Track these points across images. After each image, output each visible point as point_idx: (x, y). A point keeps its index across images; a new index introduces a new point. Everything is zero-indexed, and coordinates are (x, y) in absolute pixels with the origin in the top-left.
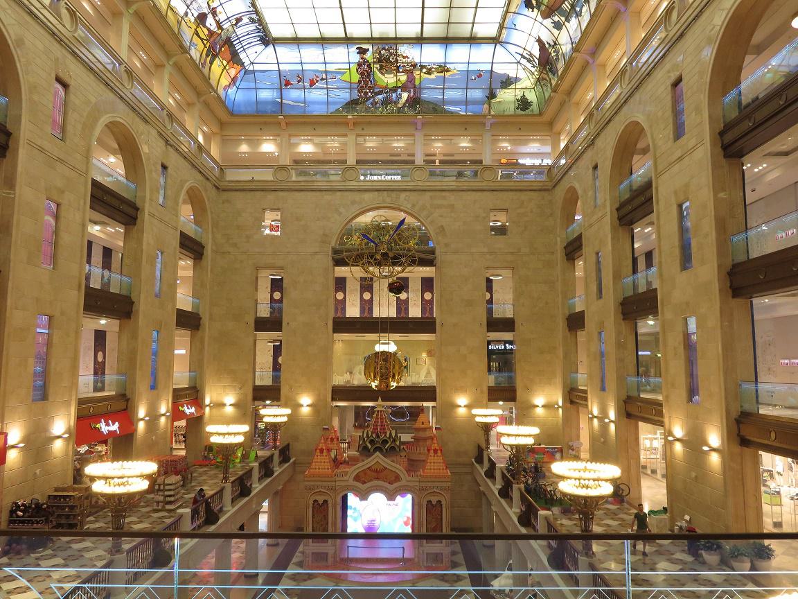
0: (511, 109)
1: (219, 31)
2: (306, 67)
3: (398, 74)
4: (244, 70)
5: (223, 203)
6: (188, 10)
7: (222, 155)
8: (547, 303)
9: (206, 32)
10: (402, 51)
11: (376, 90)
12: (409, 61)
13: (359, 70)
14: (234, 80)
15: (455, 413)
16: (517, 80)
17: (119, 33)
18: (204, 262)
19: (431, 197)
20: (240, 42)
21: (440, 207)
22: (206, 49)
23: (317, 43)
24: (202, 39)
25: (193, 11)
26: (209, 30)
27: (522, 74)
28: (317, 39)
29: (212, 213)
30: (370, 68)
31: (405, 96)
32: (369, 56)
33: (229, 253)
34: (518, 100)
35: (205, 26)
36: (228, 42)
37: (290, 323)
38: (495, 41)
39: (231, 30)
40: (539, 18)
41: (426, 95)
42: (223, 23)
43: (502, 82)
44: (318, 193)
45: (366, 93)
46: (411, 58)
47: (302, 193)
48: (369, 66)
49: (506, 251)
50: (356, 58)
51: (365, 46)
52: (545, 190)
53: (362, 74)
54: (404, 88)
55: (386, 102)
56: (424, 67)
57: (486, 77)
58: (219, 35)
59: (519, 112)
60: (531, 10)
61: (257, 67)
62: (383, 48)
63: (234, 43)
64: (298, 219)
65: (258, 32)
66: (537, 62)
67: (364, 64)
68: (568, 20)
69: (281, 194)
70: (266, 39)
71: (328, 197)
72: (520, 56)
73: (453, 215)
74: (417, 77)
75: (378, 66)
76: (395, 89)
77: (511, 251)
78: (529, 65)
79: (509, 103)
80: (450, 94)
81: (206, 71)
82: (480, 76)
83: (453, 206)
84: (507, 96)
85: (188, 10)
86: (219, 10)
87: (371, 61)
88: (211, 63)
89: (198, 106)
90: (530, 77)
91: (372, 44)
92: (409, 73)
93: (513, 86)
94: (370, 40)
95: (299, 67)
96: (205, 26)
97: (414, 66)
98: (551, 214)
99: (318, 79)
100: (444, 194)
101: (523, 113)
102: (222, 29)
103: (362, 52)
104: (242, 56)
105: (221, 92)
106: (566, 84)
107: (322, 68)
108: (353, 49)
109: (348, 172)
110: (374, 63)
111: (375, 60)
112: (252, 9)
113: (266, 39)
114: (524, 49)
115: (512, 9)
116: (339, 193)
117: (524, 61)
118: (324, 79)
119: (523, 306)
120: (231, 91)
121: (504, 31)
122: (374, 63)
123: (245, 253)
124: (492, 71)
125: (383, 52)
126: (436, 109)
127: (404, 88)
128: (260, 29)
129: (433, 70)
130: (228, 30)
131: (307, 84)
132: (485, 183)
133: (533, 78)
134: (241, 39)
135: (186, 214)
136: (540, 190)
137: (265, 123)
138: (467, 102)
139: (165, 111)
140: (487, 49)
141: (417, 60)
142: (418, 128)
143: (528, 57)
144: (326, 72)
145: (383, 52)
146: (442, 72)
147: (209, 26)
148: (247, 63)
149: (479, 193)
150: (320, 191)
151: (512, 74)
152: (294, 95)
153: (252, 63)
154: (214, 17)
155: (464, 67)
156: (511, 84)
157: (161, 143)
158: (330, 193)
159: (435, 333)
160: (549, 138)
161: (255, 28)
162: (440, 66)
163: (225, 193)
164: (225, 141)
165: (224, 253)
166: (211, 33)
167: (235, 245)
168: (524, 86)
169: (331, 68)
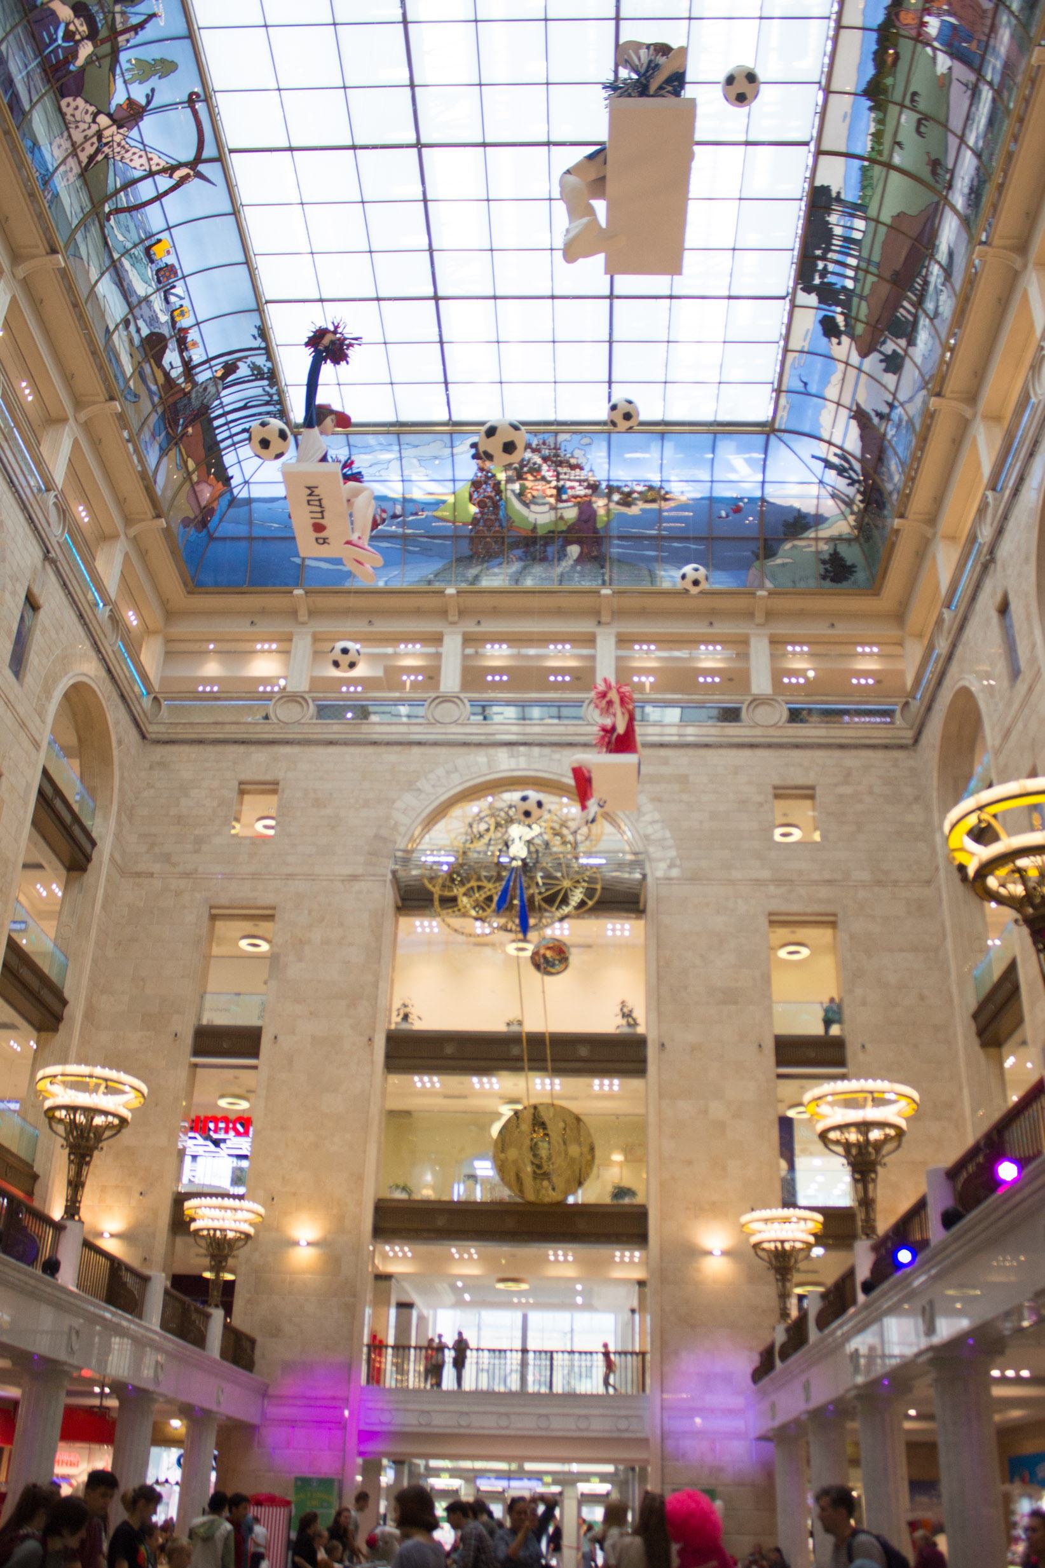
1: (188, 388)
3: (561, 505)
4: (228, 497)
5: (151, 768)
6: (130, 317)
7: (163, 680)
8: (922, 998)
9: (161, 379)
10: (569, 450)
12: (583, 475)
13: (475, 496)
16: (819, 520)
18: (89, 877)
20: (227, 424)
21: (655, 779)
23: (388, 433)
25: (141, 323)
26: (167, 375)
29: (122, 778)
33: (152, 875)
34: (824, 562)
36: (203, 416)
37: (280, 1038)
40: (855, 358)
42: (198, 370)
43: (786, 524)
44: (370, 750)
46: (587, 468)
47: (331, 750)
49: (815, 877)
50: (468, 469)
52: (901, 747)
53: (481, 504)
56: (618, 489)
58: (187, 394)
60: (834, 340)
61: (257, 492)
63: (216, 423)
64: (318, 803)
65: (267, 403)
66: (857, 466)
67: (486, 483)
68: (911, 342)
69: (287, 750)
71: (391, 756)
72: (822, 464)
73: (685, 797)
74: (601, 512)
77: (827, 875)
78: (841, 483)
82: (737, 510)
85: (130, 317)
86: (193, 335)
87: (501, 476)
90: (847, 511)
93: (811, 534)
96: (160, 365)
97: (594, 487)
98: (917, 799)
99: (384, 516)
100: (663, 752)
102: (195, 384)
104: (229, 459)
109: (440, 707)
110: (509, 480)
111: (510, 473)
112: (259, 343)
114: (830, 443)
116: (416, 751)
117: (831, 476)
118: (399, 517)
119: (864, 1003)
123: (187, 875)
128: (271, 396)
129: (635, 495)
130: (205, 389)
132: (758, 732)
133: (852, 513)
134: (230, 417)
136: (886, 747)
139: (52, 494)
142: (604, 619)
143: (836, 461)
146: (653, 501)
147: (168, 368)
149: (747, 753)
150: (375, 743)
153: (246, 482)
154: (181, 352)
156: (806, 527)
157: (37, 553)
158: (398, 749)
161: (260, 391)
162: (651, 488)
164: (169, 656)
165: (138, 875)
166: (169, 380)
167: (167, 858)
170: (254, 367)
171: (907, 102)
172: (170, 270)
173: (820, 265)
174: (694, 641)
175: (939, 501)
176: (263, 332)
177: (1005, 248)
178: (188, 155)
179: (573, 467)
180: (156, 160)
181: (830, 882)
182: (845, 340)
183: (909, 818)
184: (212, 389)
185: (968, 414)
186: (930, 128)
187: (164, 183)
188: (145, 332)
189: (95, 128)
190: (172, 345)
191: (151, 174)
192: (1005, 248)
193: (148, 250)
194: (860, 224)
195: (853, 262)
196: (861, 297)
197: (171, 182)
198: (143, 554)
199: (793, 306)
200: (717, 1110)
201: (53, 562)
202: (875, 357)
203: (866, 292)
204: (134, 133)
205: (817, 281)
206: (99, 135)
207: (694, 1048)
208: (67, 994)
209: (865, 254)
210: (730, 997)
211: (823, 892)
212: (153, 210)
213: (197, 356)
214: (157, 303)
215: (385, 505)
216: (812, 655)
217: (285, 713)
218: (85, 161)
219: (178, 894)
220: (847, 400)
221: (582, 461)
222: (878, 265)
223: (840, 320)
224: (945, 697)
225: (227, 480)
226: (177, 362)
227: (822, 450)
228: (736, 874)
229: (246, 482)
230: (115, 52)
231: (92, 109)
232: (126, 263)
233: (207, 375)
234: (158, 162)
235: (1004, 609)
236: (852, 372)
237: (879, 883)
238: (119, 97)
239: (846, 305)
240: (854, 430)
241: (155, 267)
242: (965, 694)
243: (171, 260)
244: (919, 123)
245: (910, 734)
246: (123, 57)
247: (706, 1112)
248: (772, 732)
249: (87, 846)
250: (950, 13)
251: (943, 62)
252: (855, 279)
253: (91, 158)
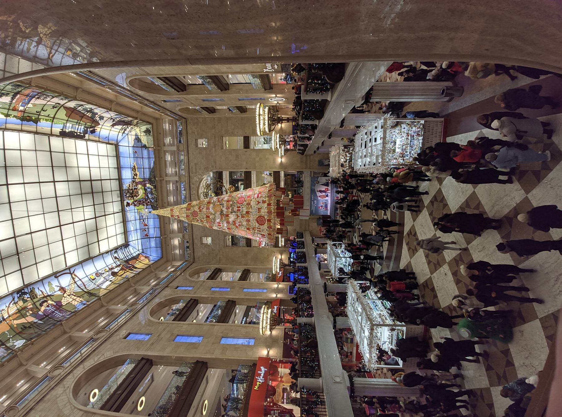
0: (151, 138)
1: (121, 266)
2: (138, 227)
7: (181, 260)
9: (121, 271)
11: (147, 198)
14: (146, 257)
16: (136, 135)
17: (115, 310)
19: (192, 173)
21: (196, 169)
22: (129, 271)
24: (124, 273)
26: (120, 270)
27: (133, 133)
28: (124, 224)
30: (136, 201)
31: (148, 185)
32: (130, 202)
33: (220, 258)
35: (118, 272)
36: (127, 261)
38: (117, 146)
39: (121, 261)
40: (100, 126)
41: (147, 176)
43: (138, 142)
45: (148, 202)
48: (135, 201)
50: (132, 207)
51: (125, 204)
52: (186, 122)
53: (140, 204)
54: (144, 186)
55: (152, 193)
57: (136, 149)
59: (151, 134)
61: (140, 248)
62: (126, 195)
66: (124, 126)
68: (97, 114)
69: (194, 237)
70: (126, 245)
74: (139, 180)
75: (135, 197)
76: (145, 190)
78: (128, 130)
79: (148, 139)
80: (146, 165)
81: (141, 270)
82: (136, 152)
83: (196, 164)
84: (145, 140)
86: (110, 267)
87: (133, 201)
88: (136, 268)
89: (157, 272)
91: (124, 201)
92: (137, 184)
93: (140, 137)
94: (122, 201)
95: (139, 231)
96: (118, 272)
97: (133, 182)
98: (197, 119)
100: (190, 168)
101: (152, 132)
102: (120, 264)
103: (128, 204)
104: (135, 255)
105: (152, 262)
106: (134, 114)
107: (138, 222)
108: (127, 208)
110: (133, 199)
113: (126, 245)
115: (97, 139)
117: (126, 132)
120: (151, 258)
121: (110, 142)
122: (133, 199)
124: (133, 147)
125: (128, 196)
126: (153, 171)
127: (144, 186)
131: (146, 227)
132: (185, 149)
135: (204, 276)
136: (187, 125)
137: (165, 244)
138: (149, 158)
140: (121, 149)
141: (131, 180)
143: (123, 131)
144: (140, 219)
145: (128, 196)
148: (138, 252)
149: (189, 152)
151: (134, 137)
152: (152, 232)
153: (138, 250)
155: (132, 160)
157: (167, 289)
159: (251, 172)
160: (164, 120)
163: (195, 259)
164: (174, 260)
165: (220, 260)
166: (122, 269)
167: (216, 255)
168: (139, 132)
169: (138, 217)
170: (115, 253)
171: (38, 114)
172: (96, 274)
173: (78, 134)
174: (165, 161)
175: (134, 110)
176: (107, 252)
177: (77, 92)
178: (70, 275)
179: (130, 186)
180: (72, 282)
181: (215, 137)
182: (95, 128)
183: (201, 121)
184: (121, 261)
185: (115, 103)
186: (45, 108)
187: (77, 279)
188: (112, 277)
189: (68, 297)
190: (113, 270)
191: (75, 282)
192: (77, 92)
193: (93, 280)
194: (68, 125)
195: (77, 126)
196: (86, 125)
197: (76, 278)
198: (157, 268)
199: (89, 140)
200: (257, 159)
201: (168, 285)
202: (100, 122)
203: (84, 123)
204: (67, 288)
205: (82, 134)
206: (69, 295)
207: (247, 163)
208: (244, 269)
209: (75, 124)
210: (237, 156)
211: (217, 139)
212: (83, 280)
213: (114, 265)
214: (104, 275)
215: (141, 223)
216: (166, 138)
217: (187, 237)
218: (76, 297)
219: (223, 253)
220: (110, 128)
221: (128, 184)
222: (78, 120)
223: (91, 129)
224: (180, 113)
225: (139, 254)
226: (117, 269)
227: (120, 134)
229: (138, 250)
230: (49, 296)
231: (63, 298)
232: (97, 284)
233: (118, 262)
234: (72, 281)
235: (165, 101)
236: (103, 127)
237: (215, 128)
238: (59, 293)
239: (87, 128)
240: (116, 127)
241: (97, 278)
242: (179, 110)
243: (94, 274)
244: (43, 111)
245: (183, 119)
246: (49, 294)
248: (185, 147)
249: (217, 270)
250: (19, 104)
251: (30, 105)
252: (81, 126)
253: (75, 296)
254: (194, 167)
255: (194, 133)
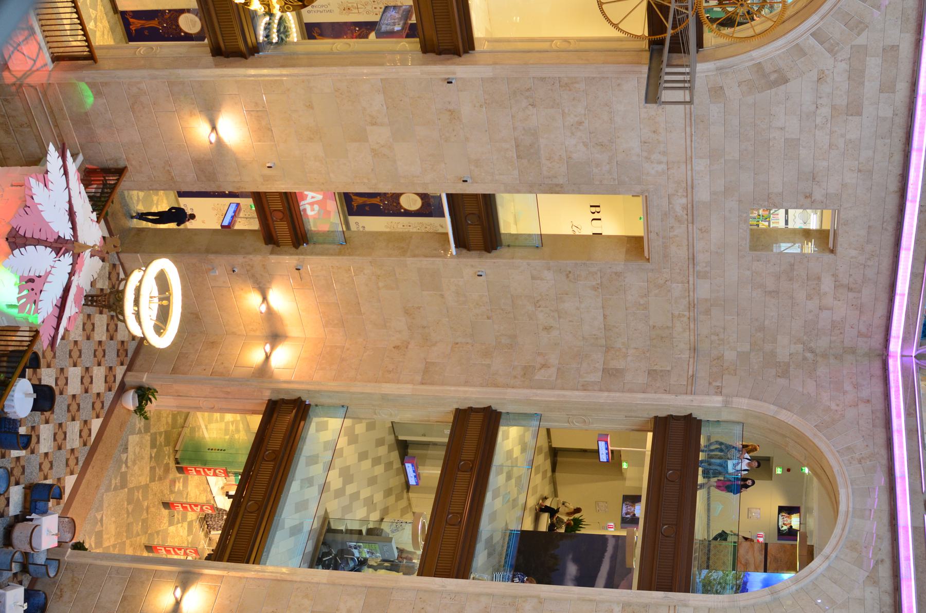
8: (547, 329)
15: (192, 114)
21: (856, 76)
49: (699, 246)
73: (825, 111)
77: (700, 257)
83: (854, 109)
181: (692, 259)
207: (453, 114)
211: (679, 252)
228: (701, 165)
237: (692, 306)
247: (374, 124)
254: (871, 87)
255: (838, 286)
